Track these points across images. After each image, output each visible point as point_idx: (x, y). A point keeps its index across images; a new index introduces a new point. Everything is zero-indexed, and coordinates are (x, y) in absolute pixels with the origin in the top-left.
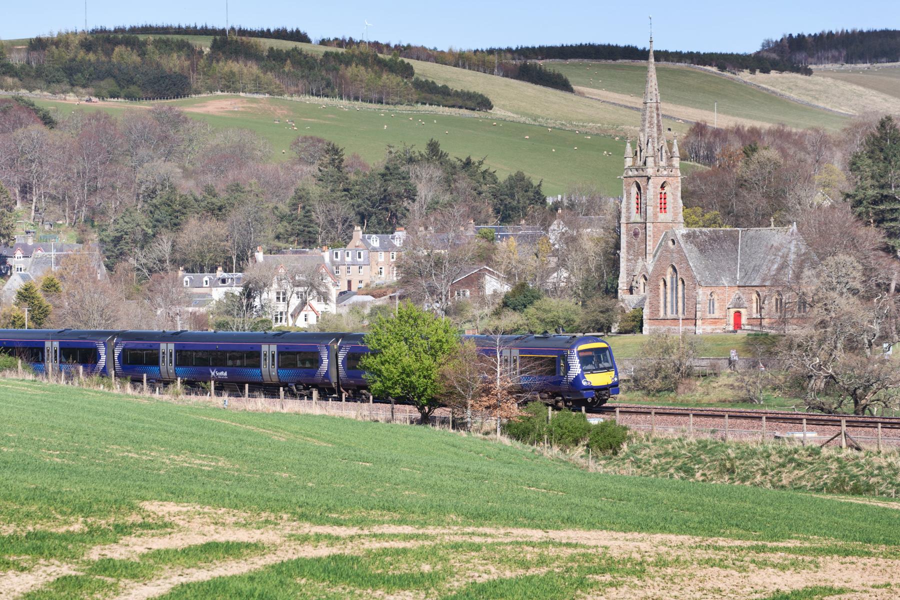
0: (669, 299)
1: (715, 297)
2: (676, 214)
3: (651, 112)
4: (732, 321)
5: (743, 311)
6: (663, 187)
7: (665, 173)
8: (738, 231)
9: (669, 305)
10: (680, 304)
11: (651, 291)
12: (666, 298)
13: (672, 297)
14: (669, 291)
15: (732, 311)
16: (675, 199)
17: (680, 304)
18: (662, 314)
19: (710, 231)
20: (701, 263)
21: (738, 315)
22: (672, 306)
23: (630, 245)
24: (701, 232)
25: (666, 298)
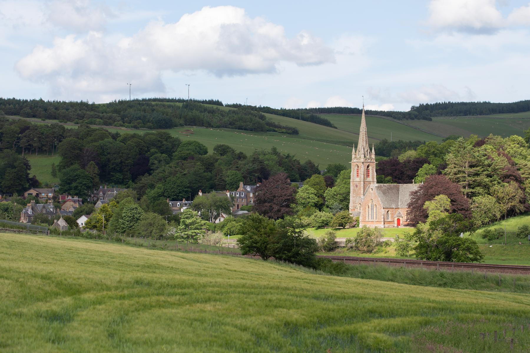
0: (370, 213)
1: (389, 212)
2: (373, 178)
3: (363, 136)
4: (396, 222)
5: (401, 218)
6: (368, 167)
7: (369, 161)
8: (399, 185)
9: (370, 216)
10: (375, 215)
11: (363, 210)
12: (369, 213)
13: (371, 212)
14: (370, 210)
15: (396, 218)
16: (373, 172)
17: (375, 215)
18: (367, 220)
19: (387, 185)
20: (384, 198)
21: (399, 220)
22: (372, 216)
23: (354, 190)
24: (384, 185)
25: (369, 213)
